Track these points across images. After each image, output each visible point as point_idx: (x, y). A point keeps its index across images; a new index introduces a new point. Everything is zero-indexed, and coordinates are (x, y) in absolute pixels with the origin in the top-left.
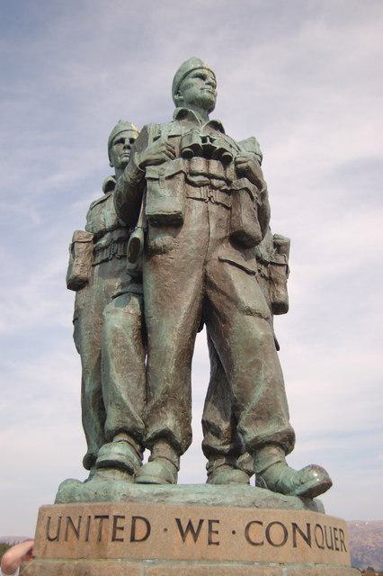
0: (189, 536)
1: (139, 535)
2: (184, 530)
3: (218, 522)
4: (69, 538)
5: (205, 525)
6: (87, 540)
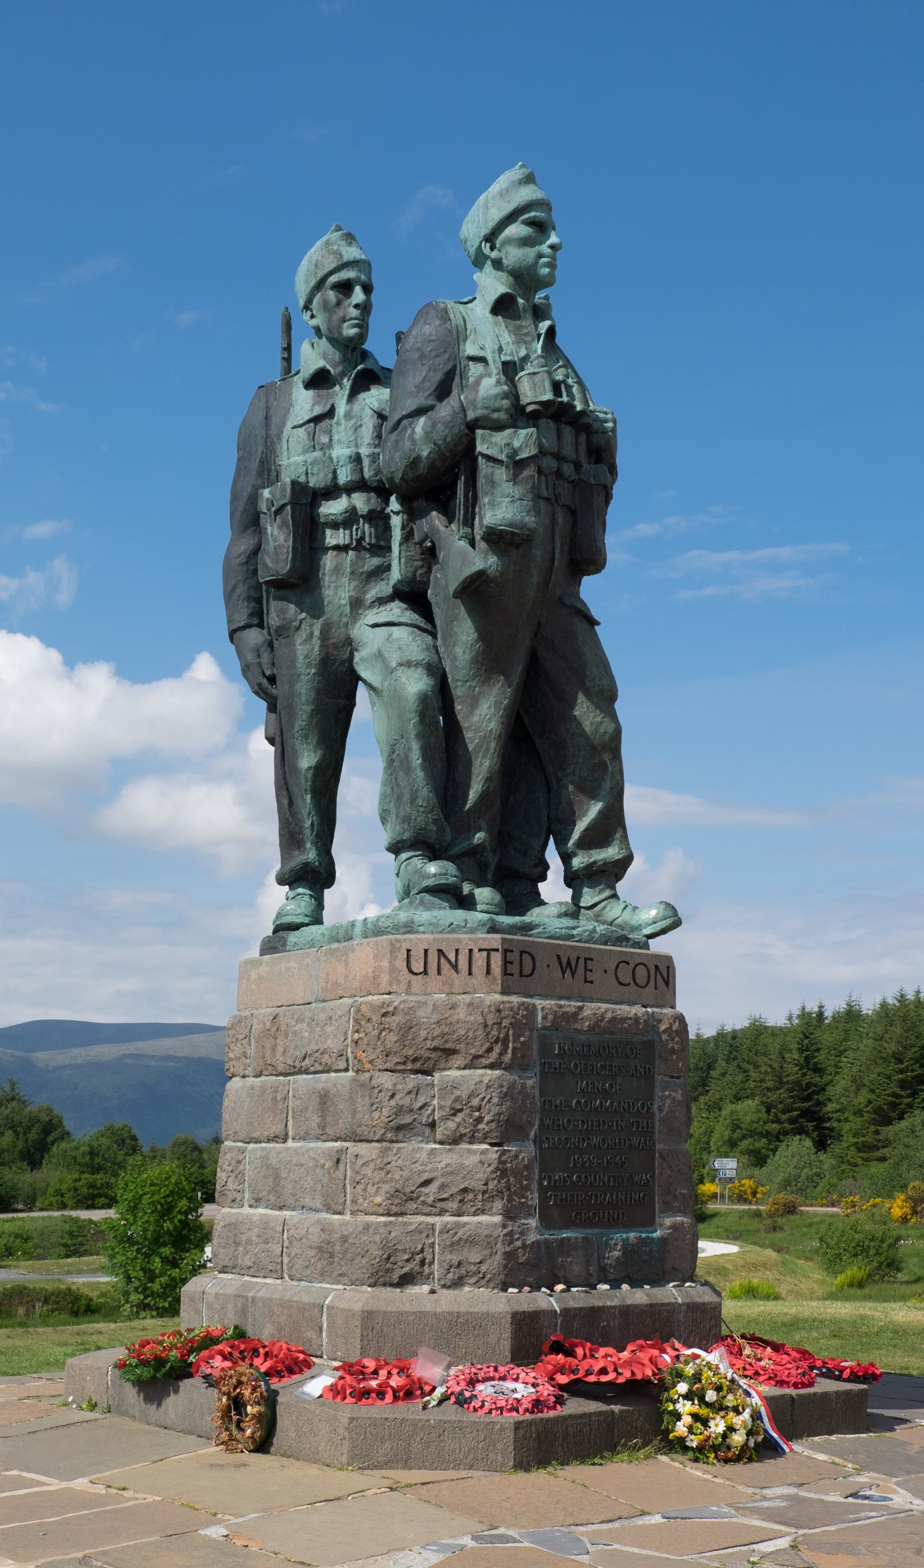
0: (568, 973)
1: (527, 970)
2: (564, 966)
3: (592, 960)
4: (443, 972)
5: (581, 961)
6: (470, 973)
